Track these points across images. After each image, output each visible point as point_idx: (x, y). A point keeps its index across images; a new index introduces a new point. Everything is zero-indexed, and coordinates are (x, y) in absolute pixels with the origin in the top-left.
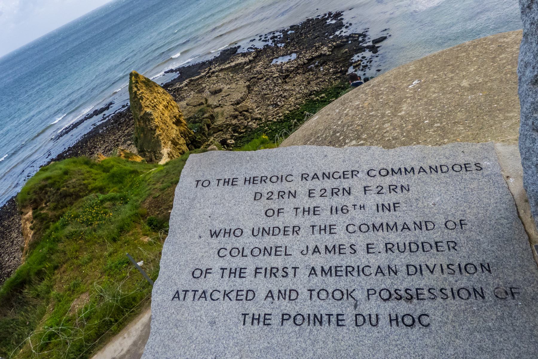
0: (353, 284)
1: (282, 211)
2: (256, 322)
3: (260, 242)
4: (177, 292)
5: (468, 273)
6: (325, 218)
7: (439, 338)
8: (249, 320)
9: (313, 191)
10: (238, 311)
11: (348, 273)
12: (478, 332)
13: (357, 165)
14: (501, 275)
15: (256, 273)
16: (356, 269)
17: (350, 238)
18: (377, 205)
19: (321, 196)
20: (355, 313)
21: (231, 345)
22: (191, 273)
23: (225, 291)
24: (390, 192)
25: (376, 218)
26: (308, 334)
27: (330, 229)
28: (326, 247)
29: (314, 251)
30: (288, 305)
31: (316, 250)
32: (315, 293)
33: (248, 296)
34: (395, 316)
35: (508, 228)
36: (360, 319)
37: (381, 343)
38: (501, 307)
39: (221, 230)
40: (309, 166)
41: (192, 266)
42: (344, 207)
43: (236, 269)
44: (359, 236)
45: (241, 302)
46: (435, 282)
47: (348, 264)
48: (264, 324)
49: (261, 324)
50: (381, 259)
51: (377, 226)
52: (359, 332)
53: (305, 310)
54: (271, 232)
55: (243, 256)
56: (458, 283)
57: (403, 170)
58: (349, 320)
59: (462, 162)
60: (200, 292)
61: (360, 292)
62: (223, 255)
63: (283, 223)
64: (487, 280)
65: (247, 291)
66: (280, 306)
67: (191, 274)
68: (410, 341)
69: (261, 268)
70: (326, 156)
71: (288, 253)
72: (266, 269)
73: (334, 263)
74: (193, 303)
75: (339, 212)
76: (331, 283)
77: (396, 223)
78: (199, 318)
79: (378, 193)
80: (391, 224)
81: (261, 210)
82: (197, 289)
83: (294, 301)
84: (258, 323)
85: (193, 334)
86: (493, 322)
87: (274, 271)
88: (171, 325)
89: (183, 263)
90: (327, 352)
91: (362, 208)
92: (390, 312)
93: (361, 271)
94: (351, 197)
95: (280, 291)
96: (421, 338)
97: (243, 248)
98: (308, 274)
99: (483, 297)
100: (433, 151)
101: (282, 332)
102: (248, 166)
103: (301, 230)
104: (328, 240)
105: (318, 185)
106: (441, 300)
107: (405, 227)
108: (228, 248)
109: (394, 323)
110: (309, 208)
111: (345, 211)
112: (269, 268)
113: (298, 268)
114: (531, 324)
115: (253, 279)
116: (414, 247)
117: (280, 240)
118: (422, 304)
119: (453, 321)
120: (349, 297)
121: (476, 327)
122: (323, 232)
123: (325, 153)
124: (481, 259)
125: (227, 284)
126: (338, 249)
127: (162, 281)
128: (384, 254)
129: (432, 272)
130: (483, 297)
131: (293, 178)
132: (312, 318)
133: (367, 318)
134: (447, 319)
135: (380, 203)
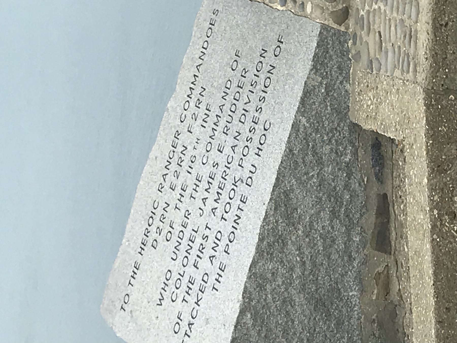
6: (191, 181)
13: (173, 129)
31: (204, 199)
55: (183, 276)
59: (207, 25)
63: (179, 226)
72: (198, 256)
94: (189, 148)
97: (179, 274)
102: (132, 246)
105: (170, 178)
123: (154, 158)
125: (192, 299)
131: (157, 201)
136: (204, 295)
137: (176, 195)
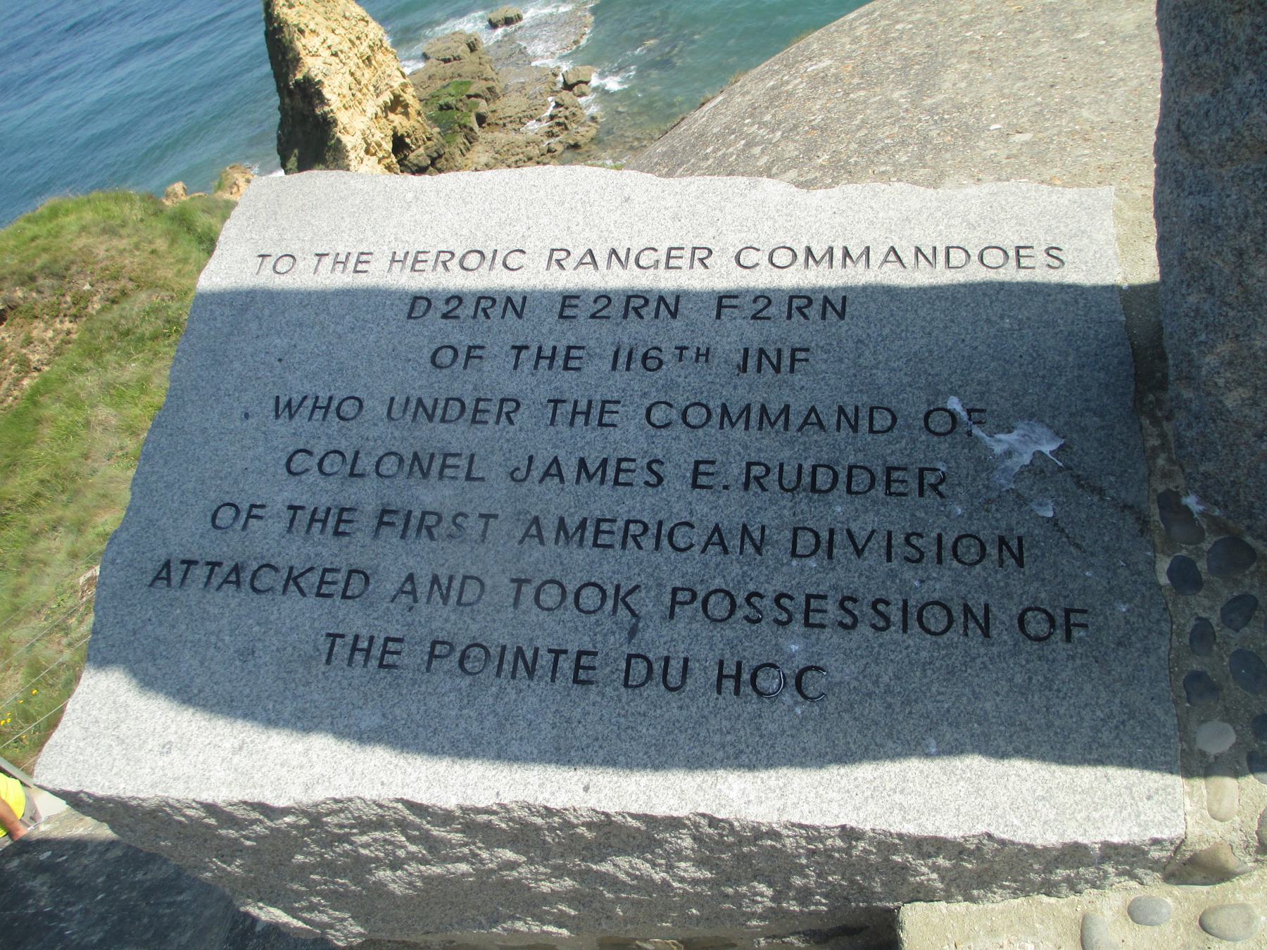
0: (637, 571)
1: (478, 352)
2: (359, 657)
3: (403, 439)
4: (167, 565)
5: (960, 561)
7: (841, 735)
8: (342, 650)
9: (574, 302)
10: (316, 624)
11: (630, 539)
12: (950, 724)
13: (712, 232)
14: (1047, 574)
15: (381, 523)
16: (653, 529)
17: (651, 440)
18: (746, 350)
19: (593, 316)
20: (628, 651)
21: (286, 715)
22: (209, 514)
23: (291, 568)
24: (790, 317)
25: (735, 388)
26: (491, 701)
27: (598, 413)
28: (582, 463)
29: (547, 474)
30: (453, 617)
32: (528, 590)
33: (351, 587)
34: (734, 668)
35: (1099, 440)
36: (640, 668)
37: (682, 738)
38: (1028, 662)
39: (305, 398)
40: (574, 228)
41: (212, 495)
42: (653, 353)
43: (329, 509)
44: (678, 438)
45: (329, 601)
46: (863, 579)
47: (634, 515)
48: (381, 666)
49: (374, 663)
50: (730, 509)
51: (734, 411)
52: (628, 704)
53: (496, 635)
54: (439, 412)
56: (925, 586)
57: (838, 254)
58: (608, 670)
60: (226, 568)
61: (653, 593)
62: (300, 469)
63: (475, 389)
64: (1007, 585)
65: (351, 572)
66: (430, 619)
67: (209, 519)
68: (761, 736)
69: (395, 512)
70: (627, 199)
71: (475, 474)
73: (596, 510)
74: (204, 597)
75: (637, 365)
76: (580, 562)
77: (787, 407)
78: (213, 639)
79: (754, 317)
80: (774, 408)
81: (421, 348)
82: (218, 559)
83: (468, 609)
84: (366, 661)
85: (192, 680)
86: (998, 699)
87: (430, 520)
88: (139, 652)
89: (190, 486)
90: (536, 751)
91: (702, 359)
92: (723, 655)
93: (664, 535)
94: (677, 323)
95: (435, 580)
96: (794, 732)
97: (357, 453)
98: (519, 534)
99: (986, 633)
100: (935, 204)
101: (423, 688)
103: (521, 410)
104: (593, 444)
106: (869, 632)
107: (812, 418)
108: (315, 451)
109: (729, 684)
110: (554, 348)
111: (652, 364)
112: (417, 514)
113: (495, 516)
114: (1099, 713)
115: (368, 541)
116: (823, 478)
117: (457, 436)
118: (814, 637)
119: (888, 691)
120: (621, 606)
121: (948, 711)
122: (580, 420)
124: (1003, 524)
126: (612, 471)
127: (132, 531)
128: (736, 494)
129: (859, 552)
130: (986, 633)
132: (509, 657)
133: (658, 667)
134: (876, 683)
135: (756, 346)
136: (312, 600)
137: (551, 331)
